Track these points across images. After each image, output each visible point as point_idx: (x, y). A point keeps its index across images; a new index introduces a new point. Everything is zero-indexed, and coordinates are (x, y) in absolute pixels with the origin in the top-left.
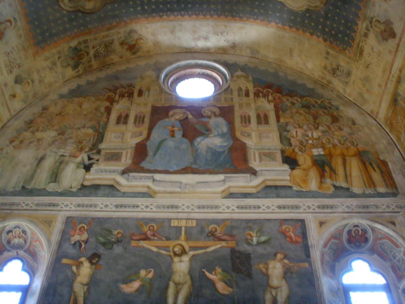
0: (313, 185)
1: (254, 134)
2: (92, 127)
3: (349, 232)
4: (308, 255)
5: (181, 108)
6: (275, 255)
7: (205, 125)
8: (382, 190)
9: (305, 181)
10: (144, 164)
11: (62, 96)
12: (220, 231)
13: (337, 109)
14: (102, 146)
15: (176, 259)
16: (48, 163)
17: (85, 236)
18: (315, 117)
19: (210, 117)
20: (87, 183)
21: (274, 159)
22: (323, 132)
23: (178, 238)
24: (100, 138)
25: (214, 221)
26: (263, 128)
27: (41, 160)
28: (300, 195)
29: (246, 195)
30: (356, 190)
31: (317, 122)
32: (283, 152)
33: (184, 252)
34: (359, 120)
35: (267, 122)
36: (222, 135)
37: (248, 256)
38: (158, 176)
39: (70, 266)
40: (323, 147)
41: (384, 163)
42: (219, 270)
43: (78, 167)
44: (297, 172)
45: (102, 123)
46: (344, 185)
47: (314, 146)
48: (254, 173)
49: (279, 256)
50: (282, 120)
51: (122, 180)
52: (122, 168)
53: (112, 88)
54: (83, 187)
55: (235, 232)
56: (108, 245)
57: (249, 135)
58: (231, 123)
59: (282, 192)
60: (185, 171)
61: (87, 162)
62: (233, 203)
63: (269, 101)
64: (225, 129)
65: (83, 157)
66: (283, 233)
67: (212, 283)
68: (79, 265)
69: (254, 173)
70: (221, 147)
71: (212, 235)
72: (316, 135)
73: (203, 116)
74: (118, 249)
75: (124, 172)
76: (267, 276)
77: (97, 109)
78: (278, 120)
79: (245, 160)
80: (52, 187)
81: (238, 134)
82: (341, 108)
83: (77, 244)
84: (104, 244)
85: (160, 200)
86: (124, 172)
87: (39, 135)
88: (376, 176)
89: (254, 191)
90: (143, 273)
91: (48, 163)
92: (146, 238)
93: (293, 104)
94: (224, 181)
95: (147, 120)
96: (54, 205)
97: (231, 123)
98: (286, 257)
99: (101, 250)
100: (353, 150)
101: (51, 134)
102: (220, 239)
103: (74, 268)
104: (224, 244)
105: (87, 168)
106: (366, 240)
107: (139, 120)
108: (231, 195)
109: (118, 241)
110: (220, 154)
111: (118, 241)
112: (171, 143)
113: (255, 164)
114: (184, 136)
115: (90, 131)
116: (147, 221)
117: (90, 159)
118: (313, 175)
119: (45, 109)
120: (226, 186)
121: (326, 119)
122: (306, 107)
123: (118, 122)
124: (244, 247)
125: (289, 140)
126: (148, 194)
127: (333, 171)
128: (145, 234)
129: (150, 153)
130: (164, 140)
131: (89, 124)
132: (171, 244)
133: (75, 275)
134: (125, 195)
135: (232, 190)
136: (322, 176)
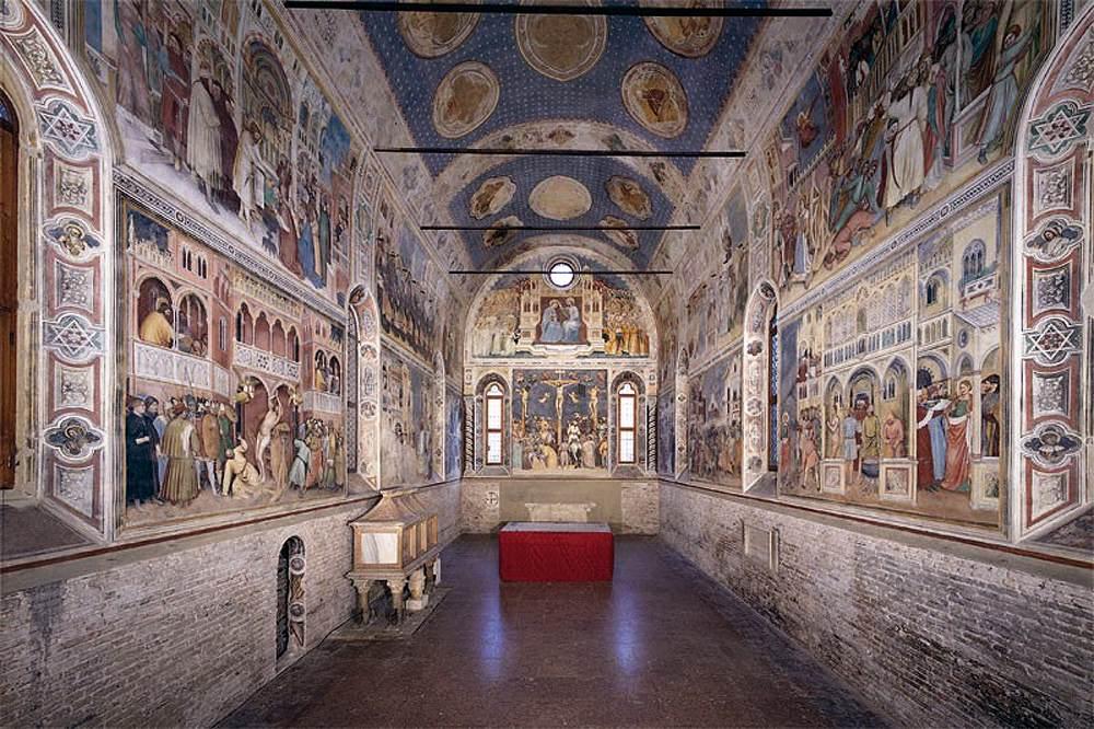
0: (614, 352)
1: (591, 319)
7: (568, 312)
8: (642, 354)
9: (610, 348)
10: (542, 339)
11: (492, 288)
12: (574, 375)
14: (520, 327)
16: (497, 338)
17: (521, 379)
21: (598, 336)
24: (518, 323)
25: (573, 371)
26: (596, 314)
27: (494, 336)
28: (607, 356)
29: (586, 357)
30: (631, 354)
34: (643, 309)
35: (598, 310)
36: (576, 320)
38: (548, 346)
41: (647, 338)
44: (608, 344)
48: (589, 344)
51: (532, 348)
52: (531, 342)
56: (532, 382)
57: (588, 320)
58: (580, 311)
59: (600, 355)
64: (577, 314)
66: (598, 377)
69: (589, 344)
71: (571, 377)
74: (536, 384)
75: (533, 344)
77: (513, 299)
79: (586, 337)
80: (502, 353)
82: (637, 298)
85: (551, 360)
88: (642, 346)
97: (580, 311)
101: (493, 319)
105: (516, 341)
108: (579, 357)
110: (573, 332)
112: (552, 325)
113: (590, 339)
114: (558, 320)
115: (512, 316)
118: (615, 344)
119: (486, 299)
121: (626, 307)
123: (525, 311)
124: (583, 383)
131: (512, 311)
133: (521, 396)
134: (535, 357)
136: (618, 346)
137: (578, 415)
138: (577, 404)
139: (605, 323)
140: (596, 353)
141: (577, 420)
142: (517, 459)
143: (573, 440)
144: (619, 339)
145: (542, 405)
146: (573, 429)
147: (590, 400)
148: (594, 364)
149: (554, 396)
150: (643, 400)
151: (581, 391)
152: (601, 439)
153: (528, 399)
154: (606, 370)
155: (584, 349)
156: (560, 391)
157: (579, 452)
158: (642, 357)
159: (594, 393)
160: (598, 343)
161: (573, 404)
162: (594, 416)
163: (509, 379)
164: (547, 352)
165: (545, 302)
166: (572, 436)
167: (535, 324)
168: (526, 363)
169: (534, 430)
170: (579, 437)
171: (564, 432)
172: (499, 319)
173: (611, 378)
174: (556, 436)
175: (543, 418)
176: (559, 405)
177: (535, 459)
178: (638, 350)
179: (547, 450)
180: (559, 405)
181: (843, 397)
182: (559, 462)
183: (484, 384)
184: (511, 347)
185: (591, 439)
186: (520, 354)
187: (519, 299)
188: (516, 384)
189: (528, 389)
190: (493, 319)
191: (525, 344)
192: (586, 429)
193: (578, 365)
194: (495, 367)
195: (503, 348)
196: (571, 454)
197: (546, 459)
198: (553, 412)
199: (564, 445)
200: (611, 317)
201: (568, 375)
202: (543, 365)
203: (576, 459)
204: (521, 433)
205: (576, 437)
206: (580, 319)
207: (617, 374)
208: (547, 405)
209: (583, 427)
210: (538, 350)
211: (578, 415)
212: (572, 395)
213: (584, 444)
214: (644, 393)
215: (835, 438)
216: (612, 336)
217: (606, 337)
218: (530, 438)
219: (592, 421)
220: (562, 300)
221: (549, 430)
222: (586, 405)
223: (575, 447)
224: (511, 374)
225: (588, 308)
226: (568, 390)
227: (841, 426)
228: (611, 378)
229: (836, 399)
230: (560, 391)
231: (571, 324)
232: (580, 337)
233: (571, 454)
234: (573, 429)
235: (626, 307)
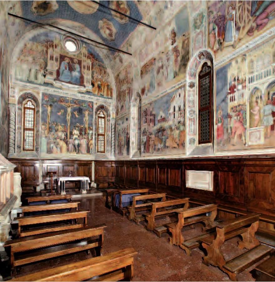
0: (96, 93)
2: (43, 59)
3: (101, 106)
4: (93, 111)
5: (68, 57)
6: (87, 110)
13: (106, 69)
15: (68, 108)
16: (33, 71)
17: (48, 99)
18: (101, 70)
19: (75, 63)
20: (45, 82)
21: (89, 83)
22: (102, 76)
23: (68, 103)
27: (30, 70)
29: (83, 93)
31: (101, 72)
32: (92, 81)
33: (69, 107)
35: (89, 70)
36: (79, 72)
37: (82, 109)
38: (63, 83)
39: (45, 107)
40: (101, 82)
42: (76, 112)
43: (42, 76)
45: (46, 58)
46: (103, 94)
47: (99, 81)
48: (85, 87)
49: (88, 110)
50: (93, 70)
51: (54, 83)
53: (47, 41)
54: (45, 83)
55: (80, 103)
56: (53, 102)
60: (70, 83)
61: (44, 74)
62: (80, 95)
63: (91, 61)
65: (42, 72)
67: (75, 115)
68: (48, 107)
69: (85, 87)
70: (78, 76)
72: (100, 77)
73: (74, 63)
74: (56, 104)
76: (85, 115)
77: (43, 51)
78: (92, 70)
80: (36, 81)
81: (82, 72)
83: (47, 101)
84: (53, 102)
86: (55, 80)
87: (27, 58)
88: (109, 93)
89: (84, 92)
90: (62, 111)
91: (33, 71)
92: (62, 102)
93: (96, 64)
94: (78, 88)
95: (59, 60)
96: (38, 88)
97: (81, 67)
98: (89, 111)
99: (52, 104)
100: (106, 85)
102: (76, 104)
103: (47, 107)
104: (77, 106)
105: (45, 76)
106: (104, 108)
107: (57, 60)
109: (56, 101)
111: (56, 101)
113: (85, 84)
114: (69, 69)
116: (62, 97)
117: (45, 73)
118: (97, 89)
119: (25, 45)
120: (79, 89)
121: (103, 71)
122: (99, 66)
123: (50, 59)
124: (82, 107)
125: (93, 77)
126: (61, 88)
127: (101, 89)
128: (61, 100)
129: (61, 75)
130: (64, 70)
132: (67, 104)
133: (47, 110)
135: (80, 91)
136: (99, 90)
137: (78, 124)
138: (78, 118)
139: (93, 77)
140: (88, 92)
141: (78, 127)
142: (44, 147)
143: (75, 139)
144: (99, 87)
145: (59, 117)
146: (76, 132)
147: (84, 116)
148: (87, 98)
149: (66, 112)
150: (109, 121)
151: (80, 111)
152: (90, 139)
153: (51, 112)
154: (93, 102)
155: (83, 89)
156: (69, 110)
157: (79, 145)
158: (109, 98)
159: (87, 113)
160: (89, 87)
161: (76, 118)
162: (87, 126)
163: (40, 97)
164: (63, 87)
165: (62, 58)
166: (75, 137)
167: (57, 68)
168: (51, 91)
169: (54, 131)
170: (79, 136)
171: (71, 133)
172: (34, 59)
173: (95, 107)
174: (66, 135)
175: (59, 124)
176: (68, 118)
177: (54, 147)
178: (108, 95)
179: (62, 143)
180: (68, 118)
181: (263, 96)
182: (68, 150)
183: (24, 97)
184: (41, 79)
185: (85, 138)
186: (46, 84)
187: (47, 52)
188: (44, 102)
189: (51, 105)
190: (30, 59)
191: (49, 79)
192: (83, 132)
193: (79, 97)
194: (30, 89)
195: (36, 78)
196: (74, 146)
197: (61, 149)
198: (65, 121)
199: (70, 140)
200: (95, 75)
201: (75, 101)
202: (61, 93)
203: (77, 148)
204: (46, 132)
205: (77, 137)
206: (80, 72)
207: (98, 105)
208: (62, 117)
209: (81, 131)
210: (57, 84)
211: (78, 124)
212: (76, 113)
213: (82, 141)
214: (110, 116)
215: (257, 117)
216: (96, 85)
217: (93, 84)
218: (51, 136)
219: (85, 129)
220: (72, 59)
221: (63, 131)
222: (82, 119)
223: (77, 142)
224: (41, 95)
225: (84, 67)
226: (74, 110)
227: (262, 111)
228: (95, 107)
229: (257, 98)
230: (69, 110)
231: (76, 74)
232: (80, 82)
233: (74, 146)
234: (76, 132)
235: (103, 71)
